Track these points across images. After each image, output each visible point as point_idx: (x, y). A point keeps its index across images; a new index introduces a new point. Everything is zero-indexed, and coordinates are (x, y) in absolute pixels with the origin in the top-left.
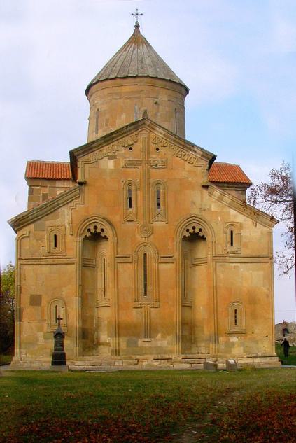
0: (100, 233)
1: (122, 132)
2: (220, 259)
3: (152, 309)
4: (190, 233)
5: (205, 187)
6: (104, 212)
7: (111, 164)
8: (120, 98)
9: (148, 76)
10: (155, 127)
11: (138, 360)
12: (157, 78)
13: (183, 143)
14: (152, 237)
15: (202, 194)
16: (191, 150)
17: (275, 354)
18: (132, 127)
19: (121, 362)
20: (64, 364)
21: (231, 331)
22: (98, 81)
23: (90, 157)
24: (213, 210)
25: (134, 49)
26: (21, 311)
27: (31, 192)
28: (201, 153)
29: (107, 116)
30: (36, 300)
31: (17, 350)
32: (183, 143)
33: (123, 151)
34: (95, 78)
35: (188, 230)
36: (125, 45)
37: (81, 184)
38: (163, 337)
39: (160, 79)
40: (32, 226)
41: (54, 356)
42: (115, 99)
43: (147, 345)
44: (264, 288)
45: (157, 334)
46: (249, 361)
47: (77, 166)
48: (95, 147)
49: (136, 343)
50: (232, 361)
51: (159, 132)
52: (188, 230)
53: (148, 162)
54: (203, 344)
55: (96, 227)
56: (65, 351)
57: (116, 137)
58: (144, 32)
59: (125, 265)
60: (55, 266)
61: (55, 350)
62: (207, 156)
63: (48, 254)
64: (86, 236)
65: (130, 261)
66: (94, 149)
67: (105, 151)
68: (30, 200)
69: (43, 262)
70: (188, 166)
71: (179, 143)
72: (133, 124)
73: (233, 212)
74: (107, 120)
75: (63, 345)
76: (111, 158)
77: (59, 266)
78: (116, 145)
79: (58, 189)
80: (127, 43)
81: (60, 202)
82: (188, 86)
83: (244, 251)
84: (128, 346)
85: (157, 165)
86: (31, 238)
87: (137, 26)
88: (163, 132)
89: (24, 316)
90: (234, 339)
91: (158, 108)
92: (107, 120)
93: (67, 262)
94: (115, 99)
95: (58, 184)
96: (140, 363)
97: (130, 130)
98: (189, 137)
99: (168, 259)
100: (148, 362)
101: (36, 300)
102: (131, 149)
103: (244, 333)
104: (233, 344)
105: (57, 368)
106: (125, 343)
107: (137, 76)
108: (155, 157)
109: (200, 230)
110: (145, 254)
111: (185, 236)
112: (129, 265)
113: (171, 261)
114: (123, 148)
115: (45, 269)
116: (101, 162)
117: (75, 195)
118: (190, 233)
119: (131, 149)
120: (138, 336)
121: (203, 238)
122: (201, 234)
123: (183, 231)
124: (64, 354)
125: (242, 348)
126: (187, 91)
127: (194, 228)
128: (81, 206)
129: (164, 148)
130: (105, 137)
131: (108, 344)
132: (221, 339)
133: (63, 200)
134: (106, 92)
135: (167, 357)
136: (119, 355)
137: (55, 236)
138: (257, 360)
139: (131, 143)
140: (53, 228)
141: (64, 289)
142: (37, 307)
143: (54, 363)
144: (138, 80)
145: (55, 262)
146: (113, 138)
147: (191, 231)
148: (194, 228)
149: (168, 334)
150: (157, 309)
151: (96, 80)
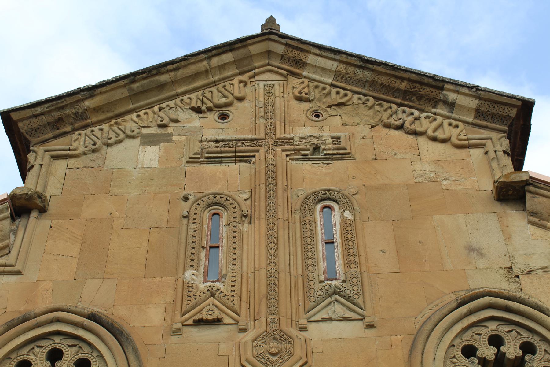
1: (193, 69)
10: (302, 56)
13: (403, 85)
15: (500, 220)
16: (435, 102)
18: (228, 57)
28: (473, 103)
32: (403, 85)
48: (97, 110)
57: (174, 83)
62: (496, 109)
85: (316, 149)
97: (222, 67)
102: (224, 117)
114: (195, 115)
128: (13, 279)
129: (339, 111)
130: (132, 77)
146: (162, 87)
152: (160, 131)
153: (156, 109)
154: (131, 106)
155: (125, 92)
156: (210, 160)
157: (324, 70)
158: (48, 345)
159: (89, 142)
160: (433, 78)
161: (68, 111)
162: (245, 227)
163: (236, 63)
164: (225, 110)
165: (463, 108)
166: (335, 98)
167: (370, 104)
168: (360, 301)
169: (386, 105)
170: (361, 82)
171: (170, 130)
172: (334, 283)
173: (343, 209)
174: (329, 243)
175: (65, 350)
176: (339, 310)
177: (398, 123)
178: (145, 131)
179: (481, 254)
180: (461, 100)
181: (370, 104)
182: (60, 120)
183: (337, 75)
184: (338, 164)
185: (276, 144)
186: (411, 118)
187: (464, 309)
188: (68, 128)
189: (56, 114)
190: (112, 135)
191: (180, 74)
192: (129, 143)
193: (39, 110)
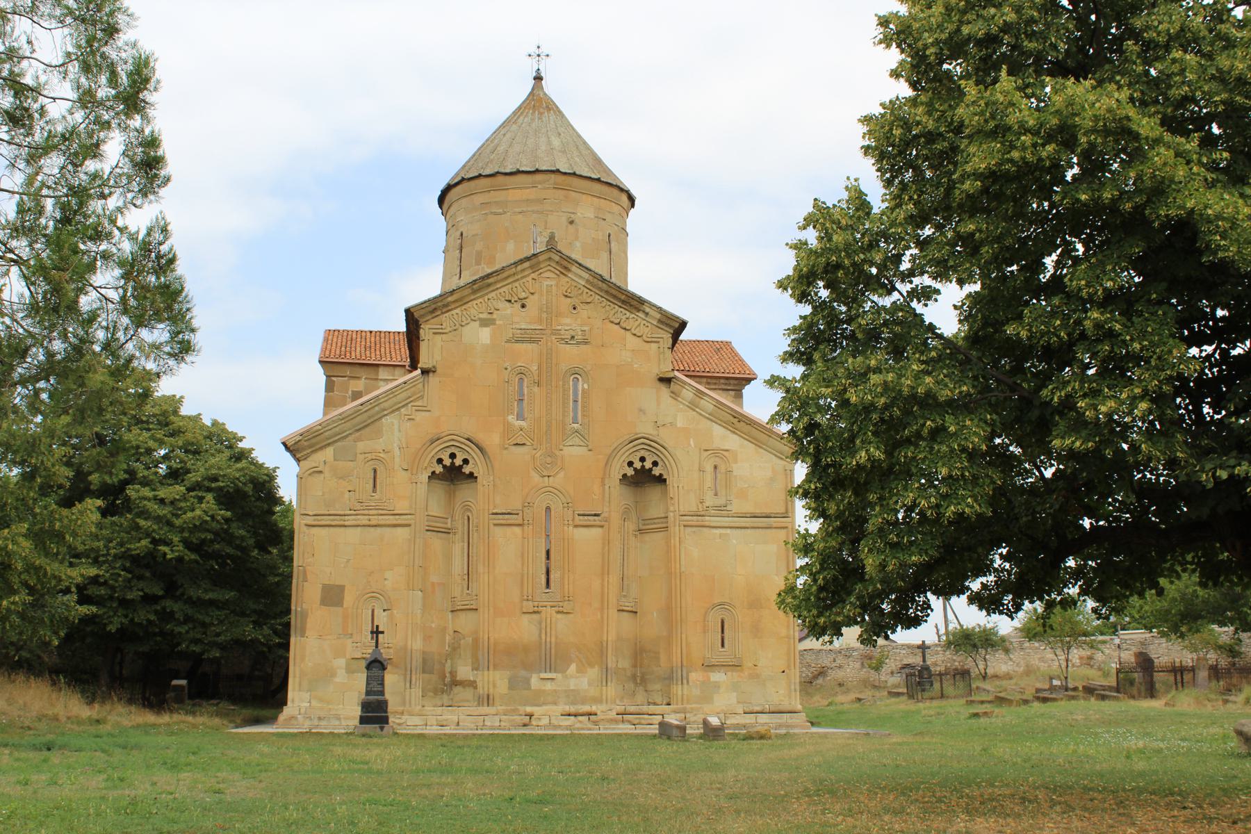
0: (461, 467)
2: (697, 520)
3: (559, 616)
4: (635, 469)
5: (666, 381)
6: (468, 427)
7: (485, 335)
8: (505, 213)
9: (558, 171)
10: (569, 266)
11: (531, 716)
12: (574, 174)
13: (623, 297)
14: (562, 474)
16: (639, 310)
17: (799, 707)
18: (527, 264)
19: (497, 718)
20: (383, 721)
21: (714, 662)
22: (463, 180)
23: (446, 320)
24: (679, 425)
25: (533, 120)
26: (304, 615)
27: (329, 387)
28: (658, 316)
29: (479, 246)
30: (333, 596)
31: (291, 694)
33: (508, 310)
34: (457, 174)
35: (630, 464)
36: (514, 113)
37: (425, 372)
38: (580, 670)
39: (581, 176)
40: (329, 451)
41: (366, 706)
42: (496, 214)
43: (549, 686)
44: (776, 578)
45: (569, 666)
46: (749, 719)
47: (418, 338)
49: (527, 681)
50: (714, 721)
51: (576, 275)
52: (630, 464)
53: (556, 332)
54: (658, 687)
55: (453, 456)
56: (388, 696)
58: (549, 86)
59: (509, 530)
60: (372, 529)
61: (368, 693)
62: (669, 322)
63: (358, 506)
64: (433, 473)
65: (521, 522)
66: (453, 306)
67: (473, 312)
68: (329, 404)
69: (350, 520)
70: (632, 341)
71: (615, 297)
72: (528, 259)
73: (718, 430)
74: (479, 254)
75: (382, 684)
76: (485, 323)
77: (379, 530)
78: (494, 299)
79: (382, 383)
80: (519, 108)
81: (386, 405)
82: (634, 192)
83: (735, 507)
84: (512, 686)
85: (573, 337)
86: (327, 474)
87: (538, 78)
88: (586, 275)
89: (308, 625)
90: (717, 677)
91: (577, 230)
92: (479, 254)
93: (395, 522)
94: (496, 214)
95: (383, 373)
96: (534, 722)
97: (523, 270)
98: (637, 283)
99: (592, 517)
100: (549, 718)
101: (333, 596)
102: (523, 306)
103: (737, 666)
104: (717, 686)
105: (370, 728)
106: (506, 681)
107: (537, 171)
108: (568, 324)
109: (655, 464)
110: (548, 509)
111: (625, 476)
112: (517, 530)
113: (598, 523)
114: (507, 304)
115: (353, 535)
116: (466, 330)
117: (414, 394)
118: (635, 469)
119: (523, 306)
120: (529, 667)
121: (661, 480)
122: (656, 471)
123: (622, 467)
124: (385, 702)
125: (735, 694)
126: (633, 206)
127: (642, 459)
129: (587, 307)
131: (473, 684)
132: (694, 676)
133: (390, 402)
134: (479, 199)
135: (586, 708)
136: (493, 705)
137: (375, 471)
138: (763, 719)
139: (523, 295)
140: (369, 456)
141: (388, 574)
142: (332, 609)
143: (363, 720)
144: (538, 177)
145: (371, 523)
146: (489, 285)
147: (638, 465)
148: (642, 459)
149: (591, 665)
150: (571, 616)
151: (459, 178)
152: (489, 316)
153: (486, 298)
154: (472, 297)
155: (468, 291)
156: (517, 341)
157: (581, 277)
158: (450, 451)
159: (452, 324)
160: (640, 298)
161: (439, 304)
162: (536, 389)
163: (531, 267)
164: (524, 301)
165: (654, 318)
166: (585, 298)
167: (604, 304)
168: (586, 437)
169: (612, 305)
170: (601, 289)
171: (494, 316)
172: (575, 425)
173: (584, 382)
174: (575, 401)
175: (457, 454)
176: (577, 441)
177: (617, 321)
178: (481, 316)
179: (644, 413)
180: (652, 313)
181: (604, 304)
182: (435, 309)
183: (588, 281)
184: (582, 347)
185: (553, 334)
186: (624, 317)
187: (631, 445)
188: (439, 313)
189: (434, 306)
190: (464, 319)
191: (499, 277)
192: (473, 324)
193: (424, 306)
